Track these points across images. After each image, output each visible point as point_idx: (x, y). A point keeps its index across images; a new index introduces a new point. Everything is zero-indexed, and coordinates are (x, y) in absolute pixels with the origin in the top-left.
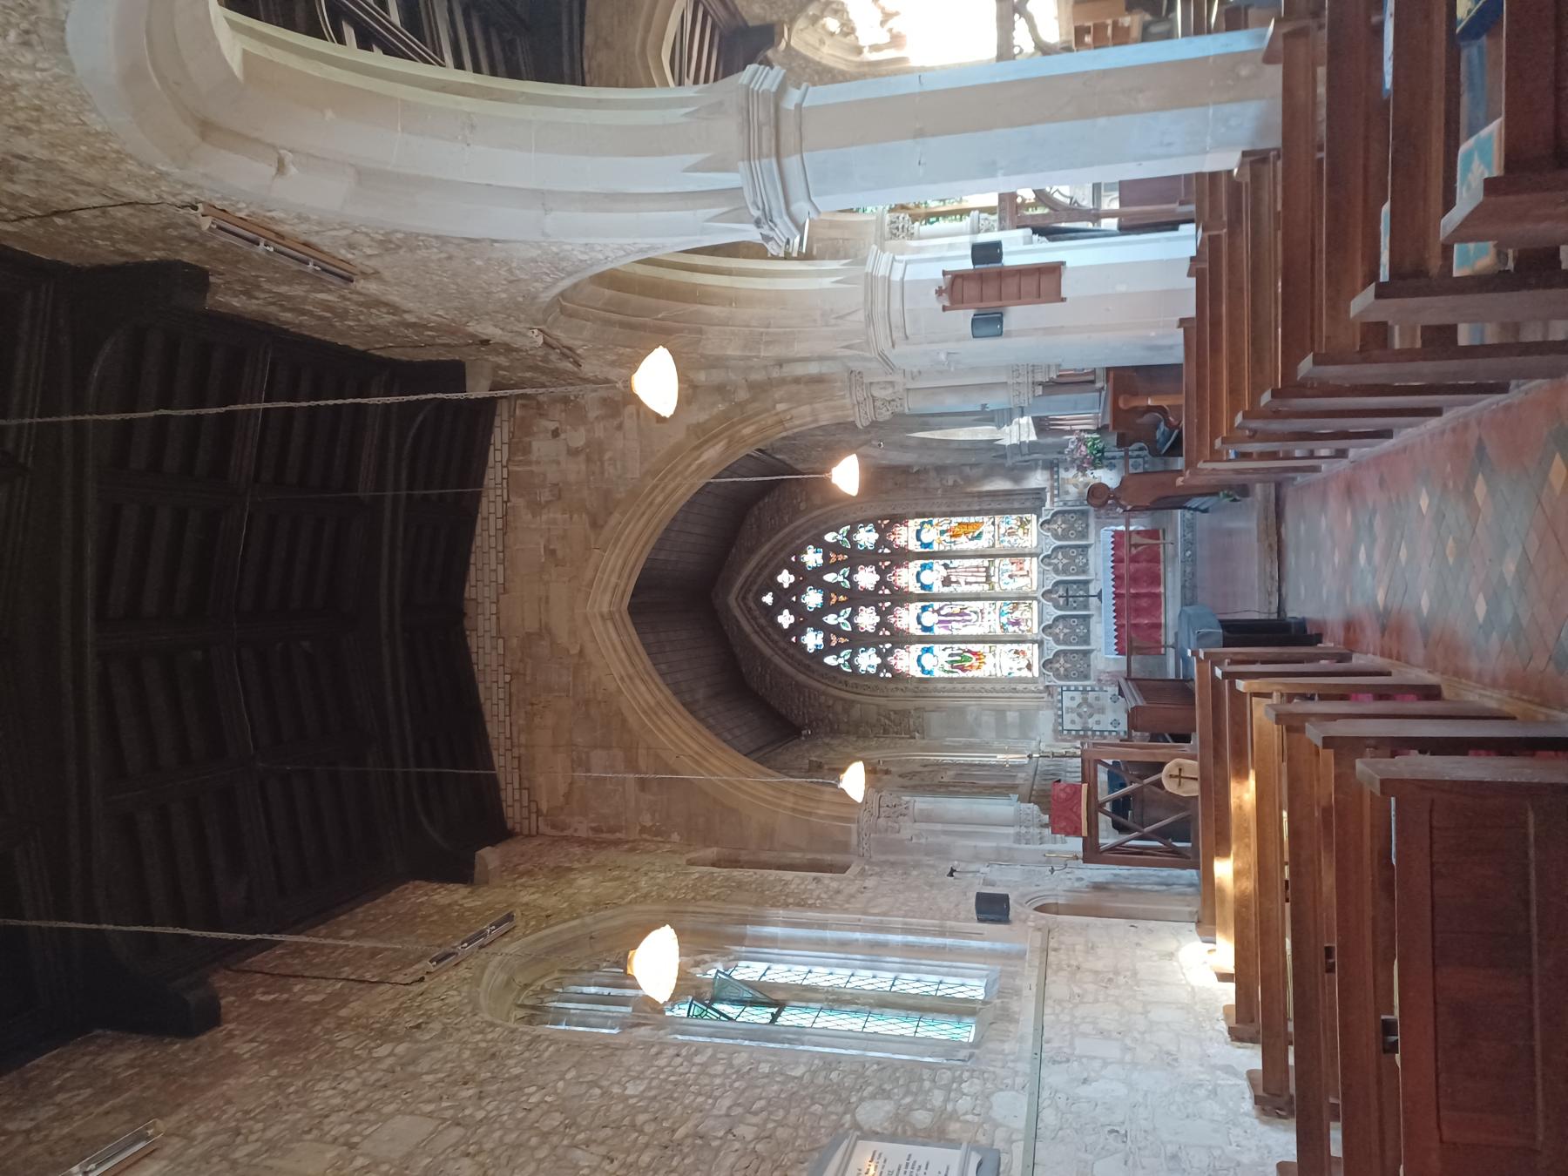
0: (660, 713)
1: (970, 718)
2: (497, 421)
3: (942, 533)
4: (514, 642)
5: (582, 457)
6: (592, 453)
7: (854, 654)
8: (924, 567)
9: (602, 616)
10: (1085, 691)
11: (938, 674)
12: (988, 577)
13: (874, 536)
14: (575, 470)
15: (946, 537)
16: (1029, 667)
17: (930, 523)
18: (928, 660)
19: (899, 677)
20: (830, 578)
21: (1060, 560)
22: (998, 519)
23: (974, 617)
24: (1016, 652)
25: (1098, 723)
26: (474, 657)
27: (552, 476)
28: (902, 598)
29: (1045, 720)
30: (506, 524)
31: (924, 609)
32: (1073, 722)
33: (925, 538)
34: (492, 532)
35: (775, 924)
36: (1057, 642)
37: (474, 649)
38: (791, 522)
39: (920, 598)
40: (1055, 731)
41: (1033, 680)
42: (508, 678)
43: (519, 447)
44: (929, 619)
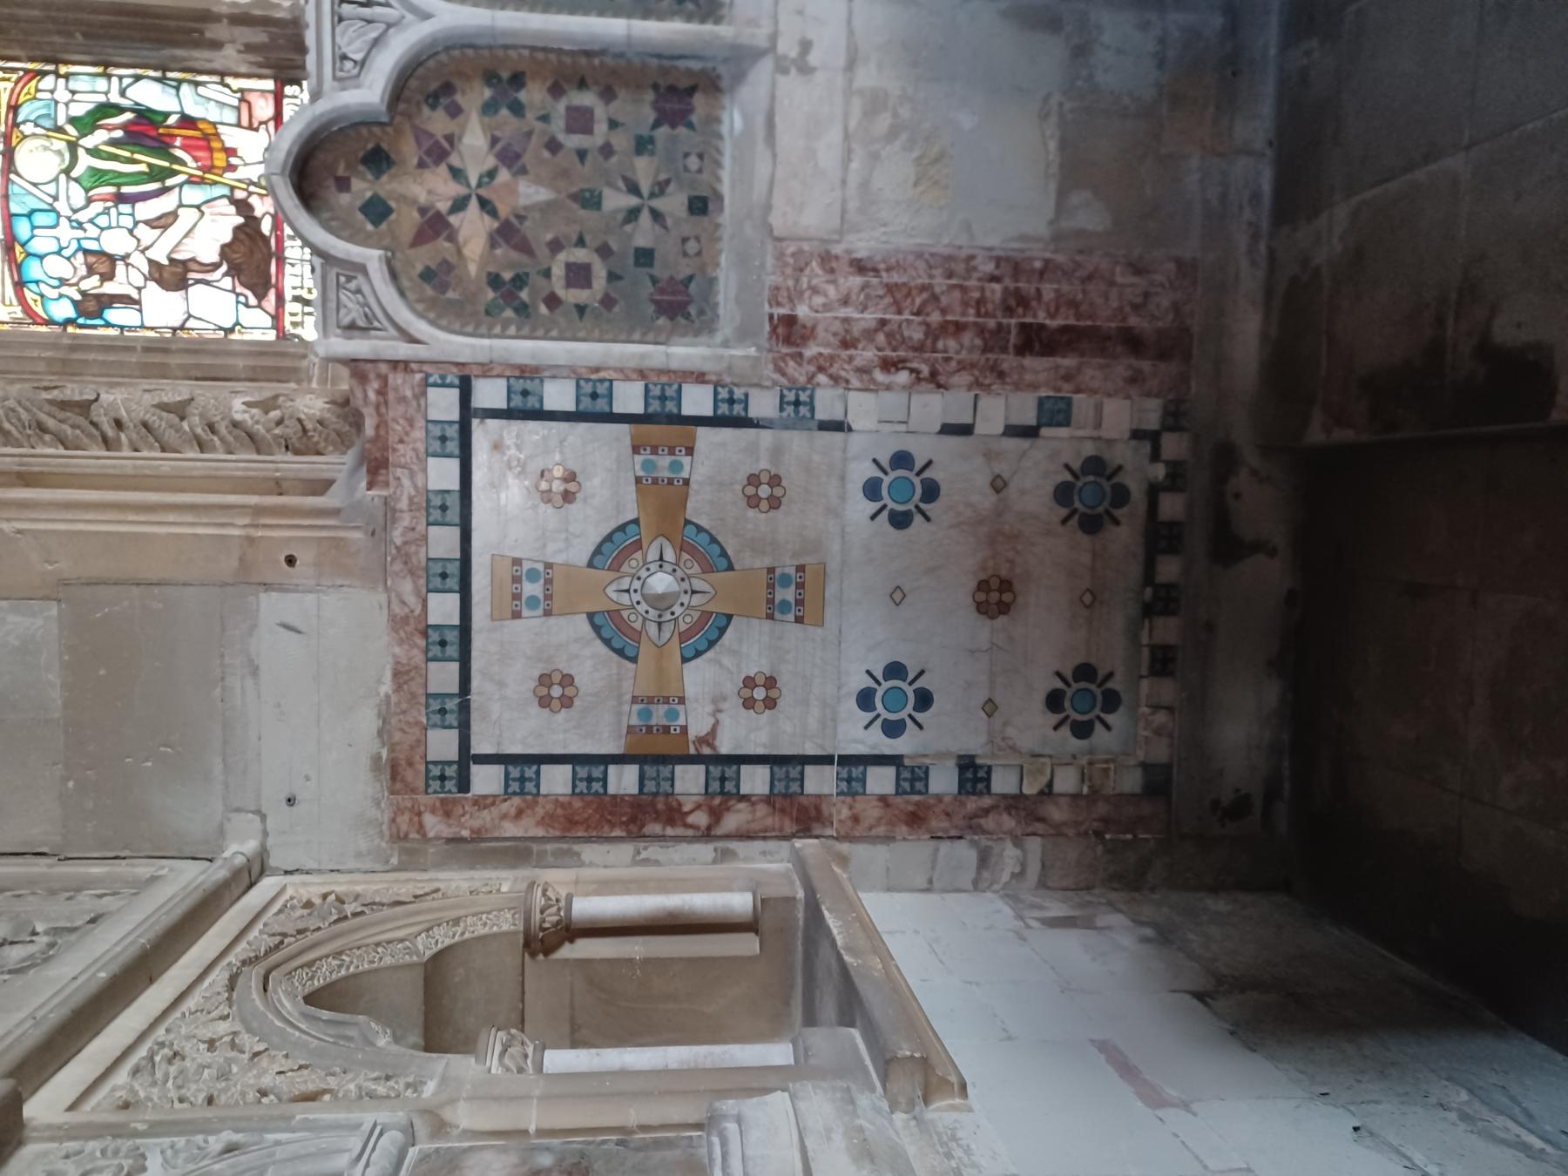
10: (662, 422)
24: (146, 131)
25: (761, 693)
29: (309, 685)
32: (555, 690)
40: (394, 772)
41: (277, 362)
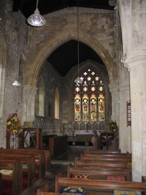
0: (51, 47)
1: (67, 108)
2: (109, 10)
3: (102, 103)
4: (65, 17)
5: (102, 28)
6: (103, 30)
7: (79, 87)
8: (95, 100)
9: (70, 34)
10: (71, 129)
11: (75, 102)
12: (93, 112)
13: (101, 90)
14: (99, 27)
15: (101, 104)
16: (76, 119)
17: (104, 101)
18: (78, 100)
19: (74, 96)
20: (93, 82)
21: (95, 125)
22: (104, 113)
23: (86, 109)
24: (79, 117)
25: (66, 131)
26: (62, 10)
27: (98, 22)
28: (89, 96)
30: (88, 14)
31: (87, 100)
32: (66, 126)
33: (101, 100)
34: (87, 11)
35: (2, 70)
36: (80, 124)
37: (64, 10)
38: (103, 74)
39: (89, 99)
42: (58, 17)
43: (104, 15)
44: (85, 101)
